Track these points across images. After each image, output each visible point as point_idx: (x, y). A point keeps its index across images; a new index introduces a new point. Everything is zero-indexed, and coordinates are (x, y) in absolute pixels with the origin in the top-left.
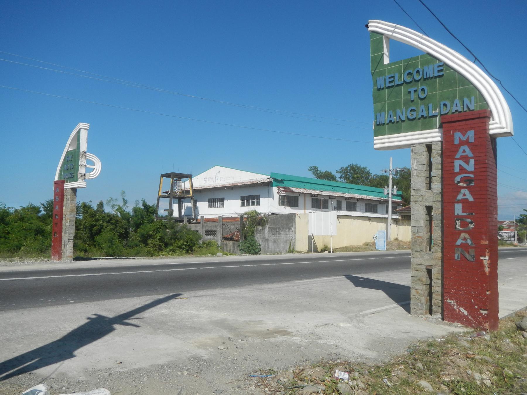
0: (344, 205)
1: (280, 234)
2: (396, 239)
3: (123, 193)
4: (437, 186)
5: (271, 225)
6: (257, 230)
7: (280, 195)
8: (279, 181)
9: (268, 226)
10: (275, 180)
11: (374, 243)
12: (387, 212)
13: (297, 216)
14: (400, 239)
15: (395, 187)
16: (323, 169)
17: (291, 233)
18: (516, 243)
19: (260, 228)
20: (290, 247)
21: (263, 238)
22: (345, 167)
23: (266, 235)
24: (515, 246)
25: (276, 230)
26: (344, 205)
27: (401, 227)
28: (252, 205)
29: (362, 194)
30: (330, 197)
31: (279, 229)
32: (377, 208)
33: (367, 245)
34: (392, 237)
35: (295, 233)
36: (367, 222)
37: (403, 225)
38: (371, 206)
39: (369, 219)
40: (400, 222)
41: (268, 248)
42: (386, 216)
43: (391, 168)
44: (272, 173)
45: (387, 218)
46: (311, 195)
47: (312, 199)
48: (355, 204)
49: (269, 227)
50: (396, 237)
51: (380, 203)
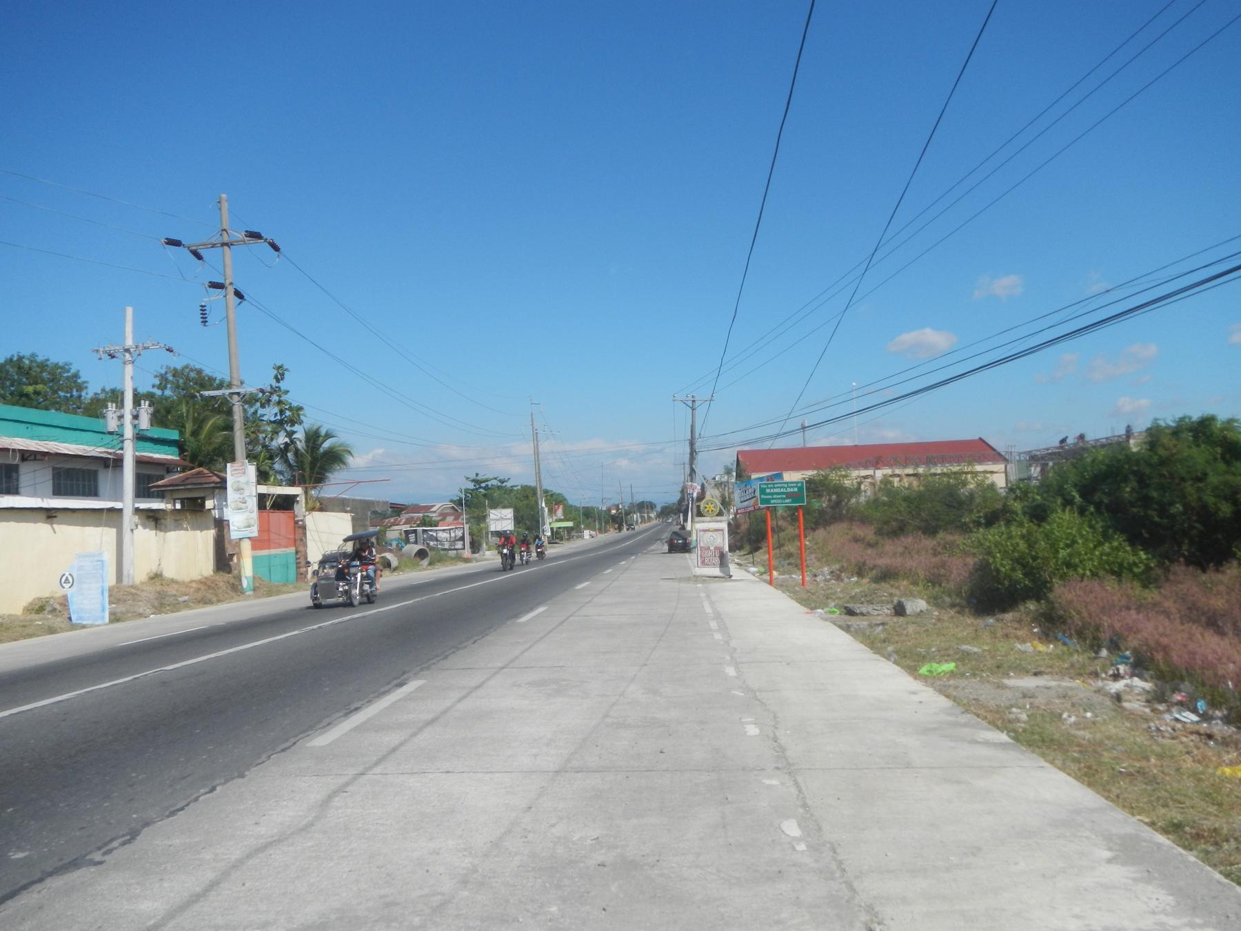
2: (156, 577)
11: (64, 602)
14: (169, 573)
15: (145, 405)
18: (467, 553)
24: (467, 560)
27: (172, 535)
29: (40, 438)
32: (96, 480)
33: (41, 609)
34: (138, 572)
36: (42, 529)
37: (178, 527)
38: (76, 476)
40: (169, 521)
42: (118, 505)
43: (129, 342)
45: (121, 510)
48: (15, 468)
50: (154, 569)
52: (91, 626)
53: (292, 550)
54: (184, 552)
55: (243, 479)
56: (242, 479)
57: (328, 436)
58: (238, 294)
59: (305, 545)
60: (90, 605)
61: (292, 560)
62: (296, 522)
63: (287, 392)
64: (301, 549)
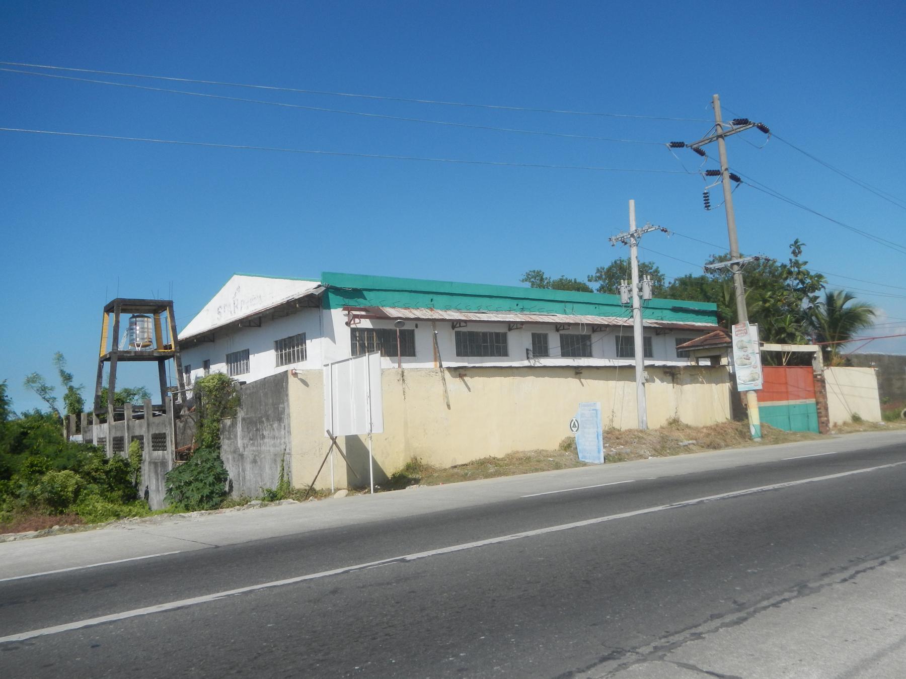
0: (554, 342)
1: (263, 437)
3: (60, 358)
7: (353, 331)
8: (351, 295)
10: (338, 291)
11: (569, 446)
12: (631, 354)
13: (291, 379)
16: (553, 274)
17: (283, 432)
20: (282, 476)
21: (235, 452)
22: (606, 267)
23: (240, 443)
26: (554, 342)
27: (688, 388)
28: (294, 362)
30: (511, 326)
35: (289, 432)
36: (572, 383)
39: (578, 371)
40: (683, 376)
41: (244, 478)
44: (324, 274)
46: (454, 324)
47: (457, 334)
48: (588, 338)
50: (673, 415)
51: (657, 334)
52: (593, 464)
53: (813, 401)
54: (701, 403)
55: (745, 338)
56: (746, 339)
57: (848, 297)
58: (734, 178)
59: (825, 397)
60: (591, 447)
61: (813, 410)
62: (815, 376)
63: (806, 263)
64: (821, 400)
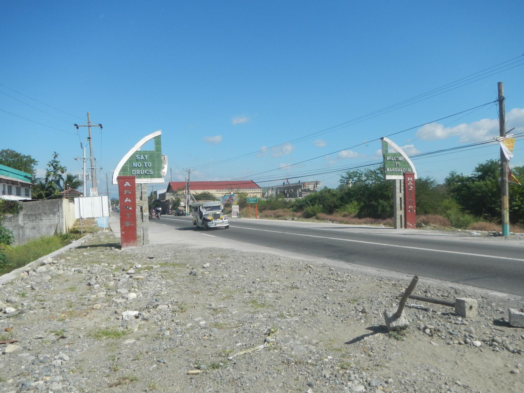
4: (403, 192)
5: (27, 211)
6: (5, 218)
9: (22, 213)
19: (9, 215)
20: (56, 231)
23: (21, 223)
25: (36, 215)
31: (40, 214)
49: (24, 214)
